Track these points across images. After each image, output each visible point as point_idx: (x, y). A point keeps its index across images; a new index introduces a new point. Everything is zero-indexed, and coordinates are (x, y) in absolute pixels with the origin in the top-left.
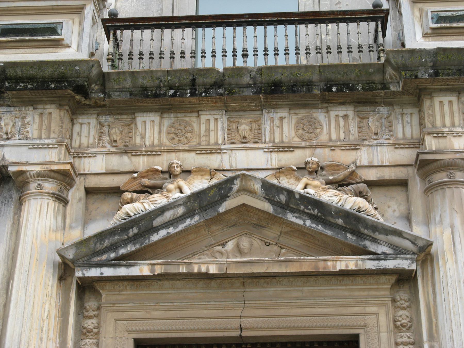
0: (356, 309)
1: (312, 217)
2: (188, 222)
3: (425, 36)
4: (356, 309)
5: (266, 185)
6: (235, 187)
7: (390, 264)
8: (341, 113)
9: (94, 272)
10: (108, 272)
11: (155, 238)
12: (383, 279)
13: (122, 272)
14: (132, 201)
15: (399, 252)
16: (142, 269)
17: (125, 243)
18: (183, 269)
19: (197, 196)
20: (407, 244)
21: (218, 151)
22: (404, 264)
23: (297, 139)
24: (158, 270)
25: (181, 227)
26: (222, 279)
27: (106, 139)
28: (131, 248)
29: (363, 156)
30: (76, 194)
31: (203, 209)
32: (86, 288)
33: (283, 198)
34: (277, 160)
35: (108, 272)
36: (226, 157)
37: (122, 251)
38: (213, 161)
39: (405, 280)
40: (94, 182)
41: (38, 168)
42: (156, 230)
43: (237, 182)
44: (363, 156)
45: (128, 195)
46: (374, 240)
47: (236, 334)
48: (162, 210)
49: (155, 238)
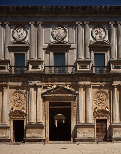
3: (80, 69)
9: (45, 96)
10: (46, 96)
11: (51, 92)
13: (48, 96)
14: (48, 88)
25: (54, 91)
28: (49, 93)
30: (42, 87)
34: (63, 84)
35: (46, 96)
37: (48, 94)
38: (56, 84)
39: (75, 97)
40: (44, 86)
45: (48, 87)
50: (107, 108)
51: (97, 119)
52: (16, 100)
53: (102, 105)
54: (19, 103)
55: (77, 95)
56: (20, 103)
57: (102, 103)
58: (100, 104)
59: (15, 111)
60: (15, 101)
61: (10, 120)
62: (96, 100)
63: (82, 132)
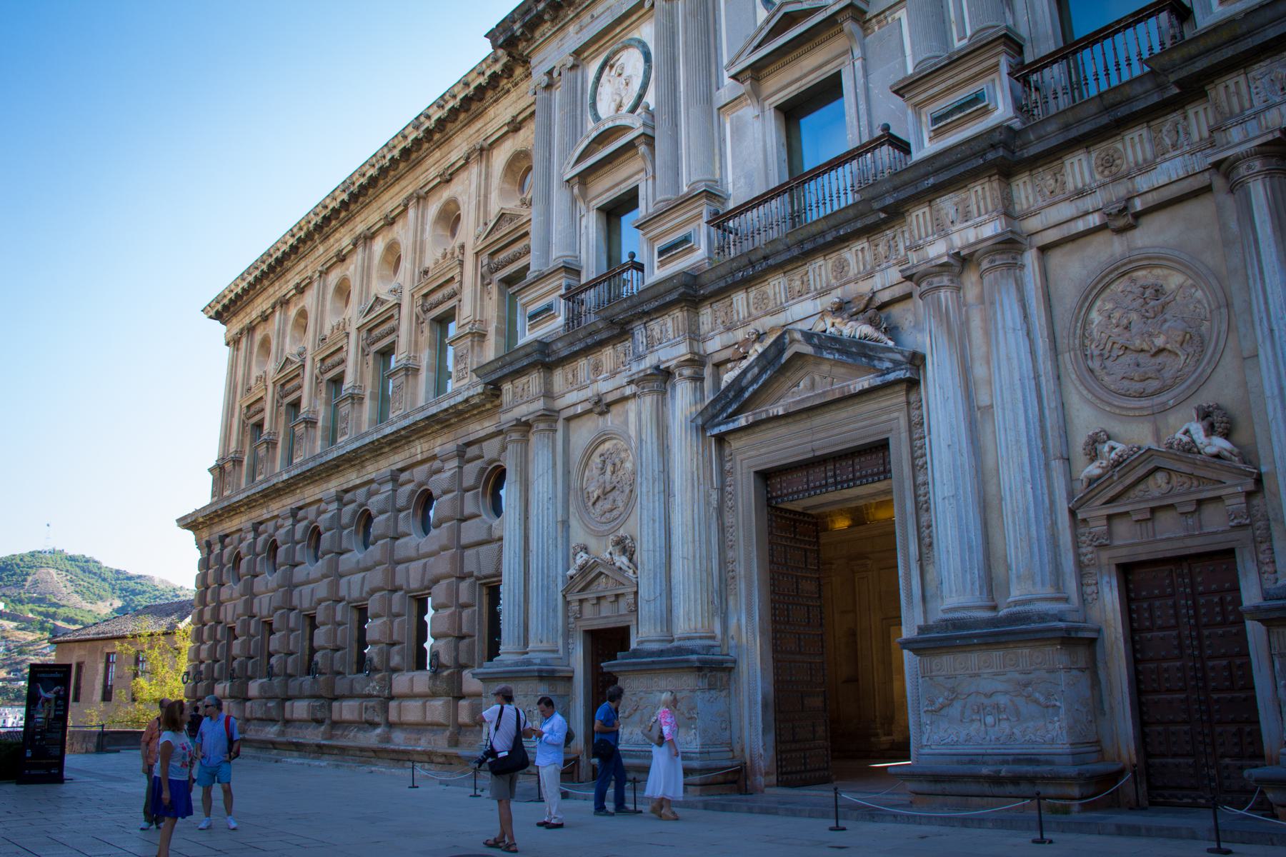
0: (885, 417)
1: (838, 350)
2: (765, 377)
4: (885, 417)
5: (804, 333)
6: (787, 341)
7: (891, 377)
8: (859, 248)
11: (747, 395)
12: (897, 388)
15: (897, 364)
16: (742, 421)
17: (730, 404)
18: (764, 416)
19: (762, 355)
20: (898, 357)
21: (783, 309)
22: (900, 374)
23: (833, 281)
24: (751, 420)
26: (787, 416)
27: (719, 321)
28: (734, 406)
29: (877, 282)
31: (771, 363)
32: (721, 439)
33: (816, 340)
36: (788, 312)
37: (730, 410)
40: (718, 358)
41: (674, 362)
42: (747, 388)
43: (787, 336)
44: (877, 282)
46: (880, 359)
47: (810, 455)
48: (744, 373)
49: (747, 395)
50: (1198, 430)
51: (1124, 555)
52: (598, 498)
53: (1157, 400)
54: (612, 510)
55: (917, 360)
56: (615, 513)
57: (1154, 385)
58: (1141, 395)
59: (583, 569)
60: (594, 504)
61: (567, 634)
62: (1095, 365)
63: (958, 705)
